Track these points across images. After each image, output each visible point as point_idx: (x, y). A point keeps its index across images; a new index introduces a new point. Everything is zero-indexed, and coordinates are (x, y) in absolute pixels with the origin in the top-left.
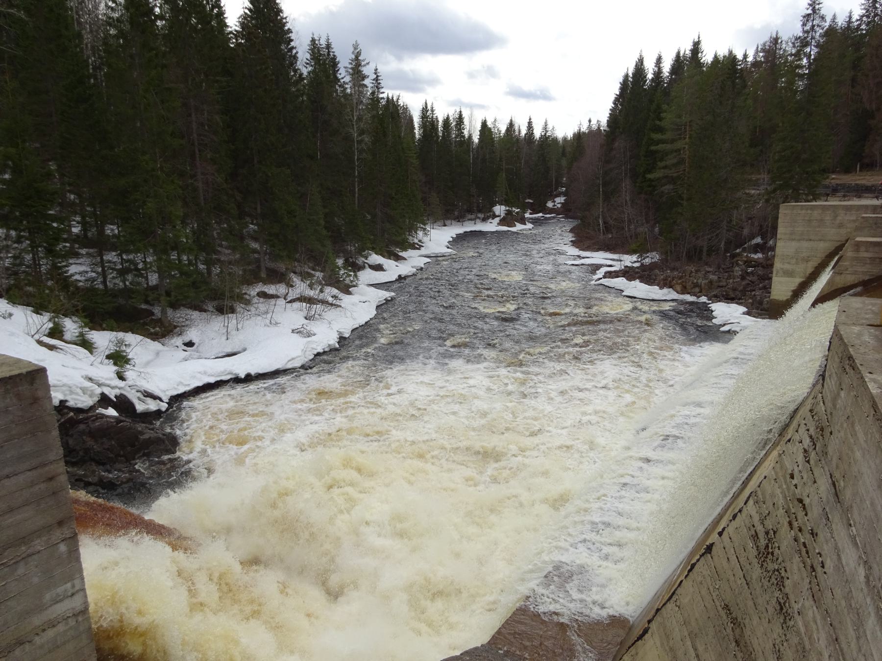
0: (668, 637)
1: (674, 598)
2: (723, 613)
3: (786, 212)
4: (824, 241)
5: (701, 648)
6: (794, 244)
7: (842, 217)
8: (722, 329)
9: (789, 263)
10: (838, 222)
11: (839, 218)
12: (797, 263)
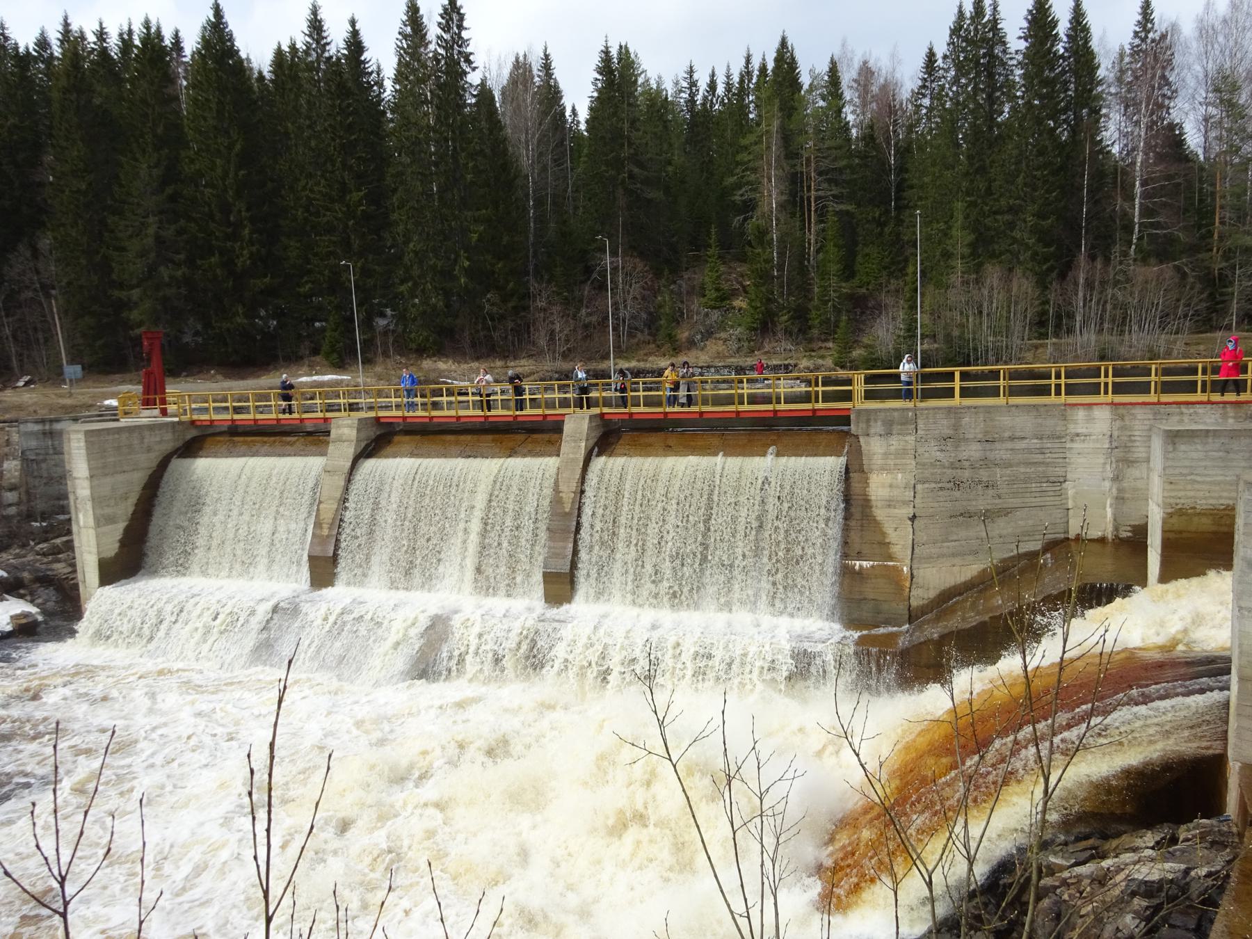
0: (931, 557)
2: (953, 519)
3: (92, 439)
4: (137, 470)
5: (955, 537)
6: (108, 480)
7: (150, 439)
9: (108, 506)
11: (146, 441)
12: (116, 504)
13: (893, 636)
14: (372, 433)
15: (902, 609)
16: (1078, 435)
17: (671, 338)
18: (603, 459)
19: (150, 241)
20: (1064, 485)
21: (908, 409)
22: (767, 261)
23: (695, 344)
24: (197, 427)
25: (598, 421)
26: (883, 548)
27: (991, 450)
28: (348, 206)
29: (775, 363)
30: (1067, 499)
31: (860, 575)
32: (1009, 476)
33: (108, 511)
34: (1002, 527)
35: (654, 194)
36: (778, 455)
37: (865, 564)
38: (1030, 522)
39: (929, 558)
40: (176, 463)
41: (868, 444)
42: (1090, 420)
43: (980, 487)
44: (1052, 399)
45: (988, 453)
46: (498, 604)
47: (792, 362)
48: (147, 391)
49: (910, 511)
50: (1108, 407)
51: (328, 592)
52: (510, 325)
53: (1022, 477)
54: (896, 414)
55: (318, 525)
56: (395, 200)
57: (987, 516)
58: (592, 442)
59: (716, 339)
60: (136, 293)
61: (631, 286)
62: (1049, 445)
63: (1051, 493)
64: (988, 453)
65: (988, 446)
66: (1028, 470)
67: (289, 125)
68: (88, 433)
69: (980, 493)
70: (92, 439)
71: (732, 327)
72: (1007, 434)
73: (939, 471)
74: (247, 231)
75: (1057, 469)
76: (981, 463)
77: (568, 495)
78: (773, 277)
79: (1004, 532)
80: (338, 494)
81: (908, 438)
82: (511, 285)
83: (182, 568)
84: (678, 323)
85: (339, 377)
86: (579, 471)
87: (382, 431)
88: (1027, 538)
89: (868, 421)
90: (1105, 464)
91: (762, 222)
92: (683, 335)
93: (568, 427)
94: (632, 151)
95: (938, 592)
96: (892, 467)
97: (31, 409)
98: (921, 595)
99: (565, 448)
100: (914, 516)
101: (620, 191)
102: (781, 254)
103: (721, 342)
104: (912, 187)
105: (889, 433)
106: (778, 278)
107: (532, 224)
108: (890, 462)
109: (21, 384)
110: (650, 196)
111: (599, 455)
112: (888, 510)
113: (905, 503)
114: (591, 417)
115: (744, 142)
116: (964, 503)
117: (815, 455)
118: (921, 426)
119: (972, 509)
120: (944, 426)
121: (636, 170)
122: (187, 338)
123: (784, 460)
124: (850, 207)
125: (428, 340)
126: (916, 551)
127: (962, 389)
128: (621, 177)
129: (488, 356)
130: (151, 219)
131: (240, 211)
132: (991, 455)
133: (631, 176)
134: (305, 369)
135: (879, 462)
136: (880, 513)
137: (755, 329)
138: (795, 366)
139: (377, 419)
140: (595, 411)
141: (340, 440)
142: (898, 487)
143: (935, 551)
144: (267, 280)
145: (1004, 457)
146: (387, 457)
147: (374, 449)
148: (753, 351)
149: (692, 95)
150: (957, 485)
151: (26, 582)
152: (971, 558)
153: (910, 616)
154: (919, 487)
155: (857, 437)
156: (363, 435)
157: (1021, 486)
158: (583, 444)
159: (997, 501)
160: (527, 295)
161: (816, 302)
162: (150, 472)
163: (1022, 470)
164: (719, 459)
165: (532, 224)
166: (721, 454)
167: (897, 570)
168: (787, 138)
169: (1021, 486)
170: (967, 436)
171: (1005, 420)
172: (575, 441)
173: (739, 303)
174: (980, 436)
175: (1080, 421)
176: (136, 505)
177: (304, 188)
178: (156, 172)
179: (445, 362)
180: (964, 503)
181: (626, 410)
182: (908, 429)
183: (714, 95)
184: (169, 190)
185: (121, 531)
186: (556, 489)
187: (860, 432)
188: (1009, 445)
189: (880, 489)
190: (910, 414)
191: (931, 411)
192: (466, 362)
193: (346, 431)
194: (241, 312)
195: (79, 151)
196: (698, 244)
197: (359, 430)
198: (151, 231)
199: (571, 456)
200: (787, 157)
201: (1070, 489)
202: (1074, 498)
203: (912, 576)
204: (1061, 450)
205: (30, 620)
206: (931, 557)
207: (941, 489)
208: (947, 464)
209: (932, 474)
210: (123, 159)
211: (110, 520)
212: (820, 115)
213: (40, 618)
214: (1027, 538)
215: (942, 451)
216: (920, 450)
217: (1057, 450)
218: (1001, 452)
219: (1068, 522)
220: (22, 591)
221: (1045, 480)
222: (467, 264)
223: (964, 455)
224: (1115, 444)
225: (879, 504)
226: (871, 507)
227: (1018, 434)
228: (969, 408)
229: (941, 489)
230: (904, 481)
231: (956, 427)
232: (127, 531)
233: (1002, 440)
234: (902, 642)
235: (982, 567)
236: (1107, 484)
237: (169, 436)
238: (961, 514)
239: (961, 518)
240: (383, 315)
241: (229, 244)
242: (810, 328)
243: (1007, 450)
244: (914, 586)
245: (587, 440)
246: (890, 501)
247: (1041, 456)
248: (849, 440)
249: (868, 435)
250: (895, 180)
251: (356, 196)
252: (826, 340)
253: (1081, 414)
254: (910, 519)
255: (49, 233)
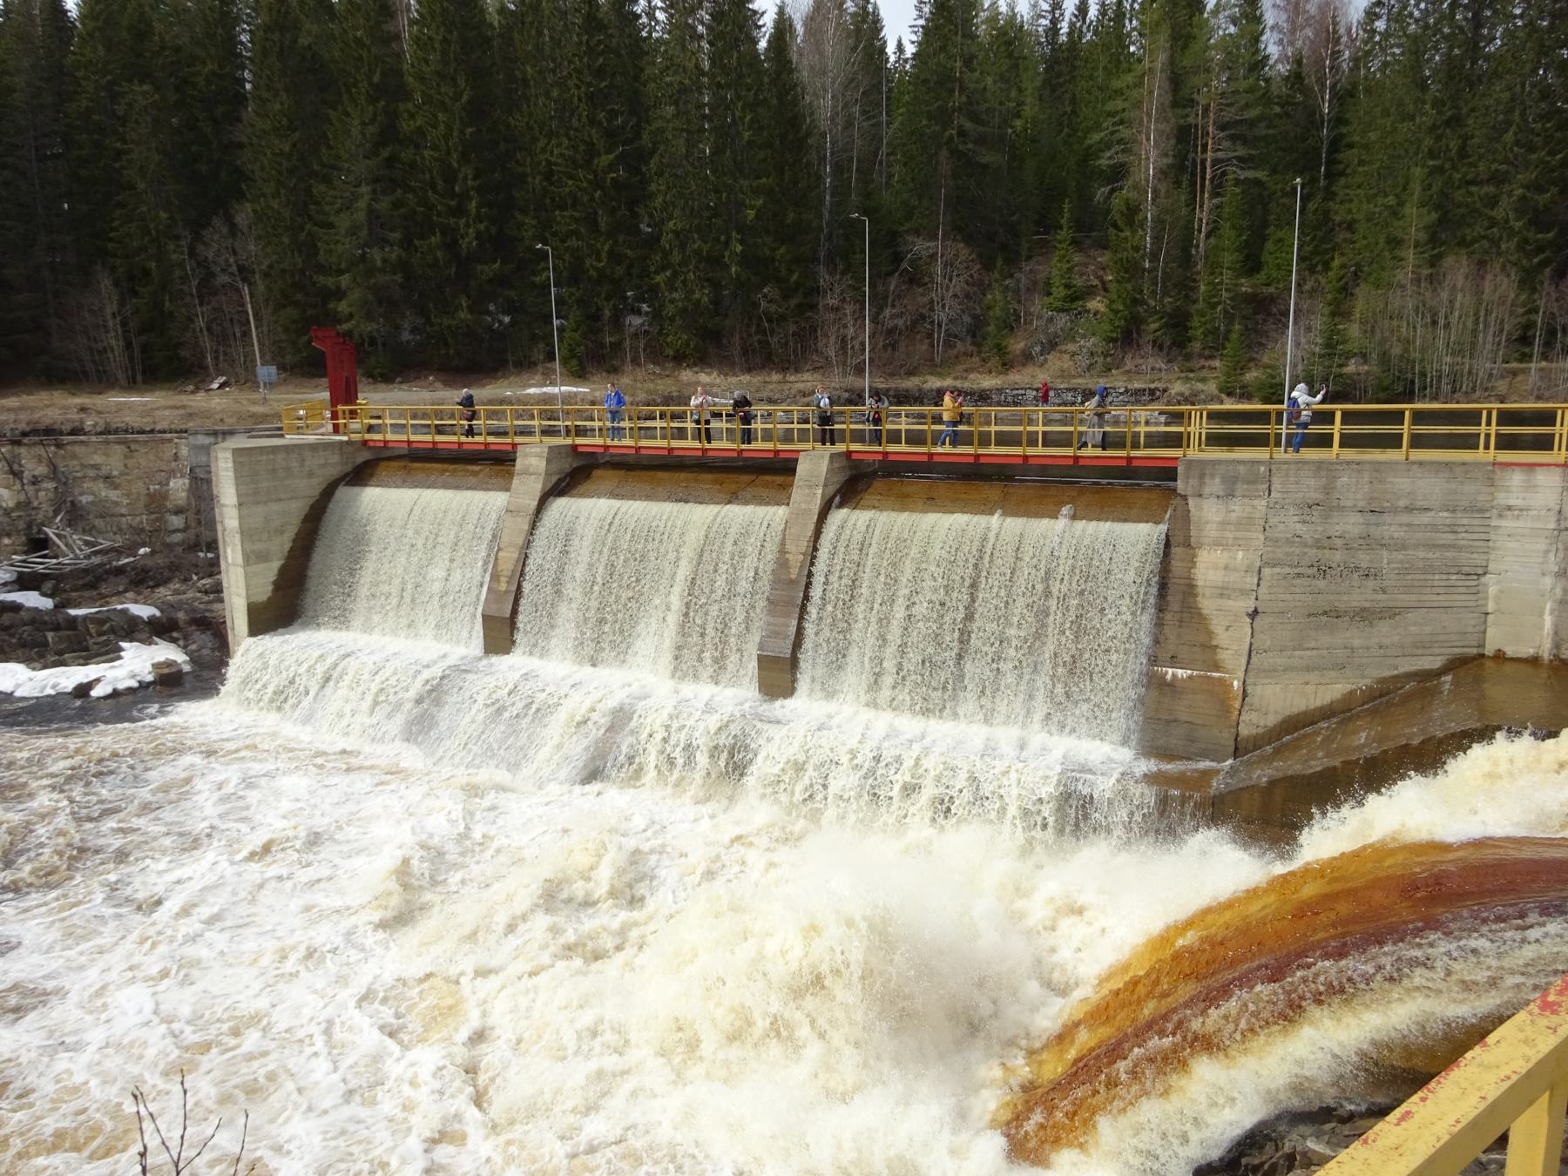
1: (1253, 653)
3: (241, 459)
5: (1313, 644)
6: (260, 509)
7: (313, 461)
8: (95, 693)
9: (260, 540)
10: (307, 469)
11: (307, 463)
13: (1207, 774)
14: (567, 465)
15: (1226, 738)
16: (1509, 508)
17: (1000, 349)
18: (844, 512)
19: (361, 216)
20: (1483, 579)
21: (1259, 462)
22: (1136, 249)
23: (1032, 358)
24: (370, 448)
25: (844, 462)
26: (1208, 652)
27: (1377, 525)
28: (595, 173)
29: (1137, 385)
30: (1486, 598)
31: (1171, 687)
32: (1401, 562)
33: (259, 546)
34: (1384, 632)
35: (988, 157)
36: (1074, 517)
37: (1180, 672)
38: (1428, 629)
39: (1271, 672)
40: (343, 492)
41: (1200, 508)
42: (1530, 487)
43: (1355, 575)
44: (1480, 455)
45: (1372, 529)
46: (702, 691)
47: (1160, 385)
48: (334, 401)
49: (1250, 604)
50: (1559, 470)
51: (502, 662)
52: (792, 328)
53: (1421, 564)
54: (1242, 468)
55: (495, 577)
56: (654, 163)
57: (1364, 616)
58: (831, 490)
59: (1061, 352)
60: (345, 280)
61: (951, 280)
62: (1465, 521)
63: (1464, 590)
64: (1372, 529)
65: (1373, 518)
66: (1430, 555)
67: (529, 69)
68: (237, 452)
69: (1356, 584)
70: (241, 459)
71: (1084, 336)
72: (1402, 503)
73: (1297, 551)
74: (474, 204)
75: (1475, 556)
76: (1361, 541)
77: (796, 558)
78: (1144, 270)
79: (1386, 641)
80: (520, 541)
81: (1256, 502)
82: (795, 277)
83: (342, 620)
84: (1012, 329)
85: (575, 389)
86: (811, 527)
87: (581, 463)
88: (1420, 652)
89: (1202, 476)
90: (1547, 552)
91: (1133, 195)
92: (1017, 345)
93: (802, 468)
94: (964, 99)
95: (1280, 718)
96: (1230, 542)
97: (218, 417)
98: (1255, 721)
99: (797, 494)
100: (1256, 612)
101: (944, 153)
102: (1157, 239)
103: (1067, 356)
104: (1350, 146)
105: (1230, 495)
106: (1150, 271)
107: (828, 197)
108: (1228, 534)
109: (215, 386)
110: (984, 160)
111: (840, 506)
112: (1220, 602)
113: (1244, 593)
114: (832, 456)
115: (1116, 84)
116: (1331, 597)
117: (1126, 520)
118: (1276, 486)
119: (1342, 606)
120: (1310, 487)
121: (968, 125)
122: (406, 336)
123: (1080, 525)
124: (1260, 174)
125: (688, 345)
126: (1254, 659)
127: (1342, 436)
128: (947, 134)
129: (763, 367)
130: (364, 189)
131: (465, 178)
132: (1376, 532)
133: (962, 133)
134: (538, 377)
135: (1213, 534)
136: (1207, 605)
137: (1114, 340)
138: (1165, 391)
139: (575, 447)
140: (841, 447)
141: (526, 472)
142: (1235, 570)
143: (1281, 661)
144: (497, 265)
145: (1396, 535)
146: (582, 496)
147: (568, 485)
148: (1110, 370)
149: (1054, 22)
150: (1322, 570)
151: (181, 624)
152: (1333, 674)
153: (1236, 749)
154: (1266, 571)
155: (1185, 498)
156: (555, 467)
157: (1417, 577)
158: (820, 491)
159: (1380, 596)
160: (815, 290)
161: (1201, 305)
162: (311, 501)
163: (1421, 554)
164: (995, 520)
165: (828, 197)
166: (999, 512)
167: (1225, 685)
168: (1176, 80)
169: (1417, 577)
170: (1342, 503)
171: (1402, 483)
172: (810, 487)
173: (1096, 304)
174: (1362, 504)
175: (1514, 489)
176: (294, 541)
177: (544, 150)
178: (371, 129)
179: (709, 374)
180: (1331, 597)
181: (880, 449)
182: (1257, 490)
183: (1084, 22)
184: (385, 153)
185: (276, 571)
186: (782, 551)
187: (1189, 491)
188: (1405, 518)
189: (1211, 572)
190: (1262, 469)
191: (1293, 466)
192: (735, 375)
193: (534, 461)
194: (464, 305)
195: (282, 104)
196: (1046, 223)
197: (549, 461)
198: (362, 204)
199: (803, 506)
200: (1175, 104)
201: (1492, 585)
202: (1497, 598)
203: (1245, 694)
204: (1483, 529)
205: (174, 670)
206: (1275, 670)
207: (1299, 575)
208: (1310, 541)
209: (1287, 554)
210: (332, 114)
211: (263, 557)
212: (1228, 45)
213: (187, 668)
214: (1420, 652)
215: (1304, 522)
216: (1273, 520)
217: (1477, 529)
218: (1391, 528)
219: (1484, 632)
220: (175, 635)
221: (1457, 569)
222: (739, 248)
223: (1336, 530)
224: (1562, 526)
225: (1208, 592)
226: (1196, 596)
227: (1419, 504)
228: (1348, 463)
229: (1299, 575)
230: (1246, 562)
231: (1328, 490)
232: (283, 571)
233: (1395, 511)
234: (1217, 785)
235: (1349, 687)
236: (1548, 581)
237: (335, 459)
238: (1325, 613)
239: (1324, 618)
240: (638, 312)
241: (452, 220)
242: (1190, 340)
243: (1401, 525)
244: (1246, 708)
245: (825, 486)
246: (1223, 588)
247: (1453, 536)
248: (1176, 501)
249: (1200, 496)
250: (1328, 136)
251: (605, 160)
252: (1211, 357)
253: (1517, 478)
254: (1248, 615)
255: (248, 205)
